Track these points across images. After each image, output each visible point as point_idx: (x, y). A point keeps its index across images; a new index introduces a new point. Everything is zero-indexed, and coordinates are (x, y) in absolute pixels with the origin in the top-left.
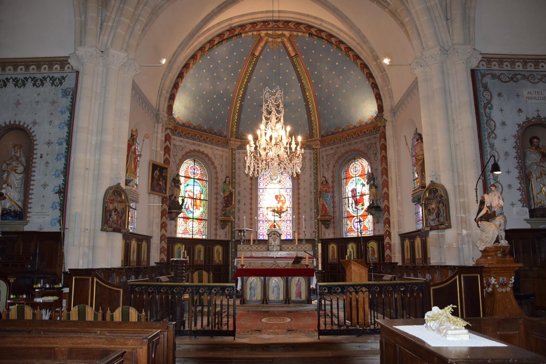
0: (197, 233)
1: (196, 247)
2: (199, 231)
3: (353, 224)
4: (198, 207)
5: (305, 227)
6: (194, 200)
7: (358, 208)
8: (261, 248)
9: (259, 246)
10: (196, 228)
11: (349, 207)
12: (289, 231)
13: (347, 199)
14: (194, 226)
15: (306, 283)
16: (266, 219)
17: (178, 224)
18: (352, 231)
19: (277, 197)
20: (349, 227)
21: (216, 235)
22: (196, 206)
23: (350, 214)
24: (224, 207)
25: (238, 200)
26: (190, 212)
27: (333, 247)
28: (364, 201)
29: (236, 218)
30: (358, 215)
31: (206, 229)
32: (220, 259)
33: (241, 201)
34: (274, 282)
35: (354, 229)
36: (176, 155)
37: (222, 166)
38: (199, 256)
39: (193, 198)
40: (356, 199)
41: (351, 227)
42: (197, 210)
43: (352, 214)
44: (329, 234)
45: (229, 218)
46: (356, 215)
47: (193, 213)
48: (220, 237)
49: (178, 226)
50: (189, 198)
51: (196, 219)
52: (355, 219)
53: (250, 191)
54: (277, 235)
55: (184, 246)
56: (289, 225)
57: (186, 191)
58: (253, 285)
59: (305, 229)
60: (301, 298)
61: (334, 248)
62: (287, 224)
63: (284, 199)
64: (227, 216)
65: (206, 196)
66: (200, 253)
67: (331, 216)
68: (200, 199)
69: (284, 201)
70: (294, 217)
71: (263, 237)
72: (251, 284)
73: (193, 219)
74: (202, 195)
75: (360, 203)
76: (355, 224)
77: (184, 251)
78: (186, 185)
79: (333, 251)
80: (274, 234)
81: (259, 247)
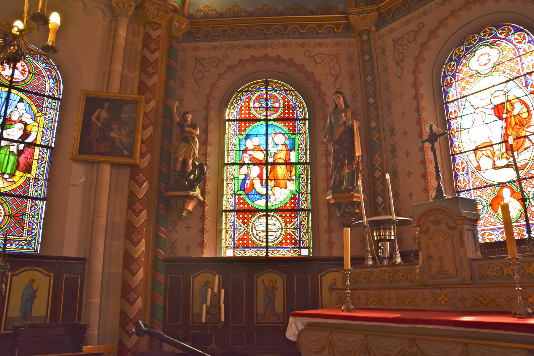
0: (281, 243)
1: (260, 279)
2: (285, 239)
4: (282, 182)
6: (269, 167)
10: (278, 234)
14: (269, 227)
16: (477, 183)
17: (223, 227)
19: (498, 110)
22: (276, 179)
31: (308, 232)
36: (201, 79)
37: (337, 77)
38: (271, 301)
49: (224, 232)
50: (254, 164)
51: (276, 211)
53: (417, 114)
54: (447, 224)
57: (245, 151)
63: (525, 110)
65: (306, 154)
66: (273, 293)
68: (287, 163)
69: (525, 115)
73: (267, 210)
74: (292, 153)
77: (216, 290)
78: (244, 136)
80: (437, 223)
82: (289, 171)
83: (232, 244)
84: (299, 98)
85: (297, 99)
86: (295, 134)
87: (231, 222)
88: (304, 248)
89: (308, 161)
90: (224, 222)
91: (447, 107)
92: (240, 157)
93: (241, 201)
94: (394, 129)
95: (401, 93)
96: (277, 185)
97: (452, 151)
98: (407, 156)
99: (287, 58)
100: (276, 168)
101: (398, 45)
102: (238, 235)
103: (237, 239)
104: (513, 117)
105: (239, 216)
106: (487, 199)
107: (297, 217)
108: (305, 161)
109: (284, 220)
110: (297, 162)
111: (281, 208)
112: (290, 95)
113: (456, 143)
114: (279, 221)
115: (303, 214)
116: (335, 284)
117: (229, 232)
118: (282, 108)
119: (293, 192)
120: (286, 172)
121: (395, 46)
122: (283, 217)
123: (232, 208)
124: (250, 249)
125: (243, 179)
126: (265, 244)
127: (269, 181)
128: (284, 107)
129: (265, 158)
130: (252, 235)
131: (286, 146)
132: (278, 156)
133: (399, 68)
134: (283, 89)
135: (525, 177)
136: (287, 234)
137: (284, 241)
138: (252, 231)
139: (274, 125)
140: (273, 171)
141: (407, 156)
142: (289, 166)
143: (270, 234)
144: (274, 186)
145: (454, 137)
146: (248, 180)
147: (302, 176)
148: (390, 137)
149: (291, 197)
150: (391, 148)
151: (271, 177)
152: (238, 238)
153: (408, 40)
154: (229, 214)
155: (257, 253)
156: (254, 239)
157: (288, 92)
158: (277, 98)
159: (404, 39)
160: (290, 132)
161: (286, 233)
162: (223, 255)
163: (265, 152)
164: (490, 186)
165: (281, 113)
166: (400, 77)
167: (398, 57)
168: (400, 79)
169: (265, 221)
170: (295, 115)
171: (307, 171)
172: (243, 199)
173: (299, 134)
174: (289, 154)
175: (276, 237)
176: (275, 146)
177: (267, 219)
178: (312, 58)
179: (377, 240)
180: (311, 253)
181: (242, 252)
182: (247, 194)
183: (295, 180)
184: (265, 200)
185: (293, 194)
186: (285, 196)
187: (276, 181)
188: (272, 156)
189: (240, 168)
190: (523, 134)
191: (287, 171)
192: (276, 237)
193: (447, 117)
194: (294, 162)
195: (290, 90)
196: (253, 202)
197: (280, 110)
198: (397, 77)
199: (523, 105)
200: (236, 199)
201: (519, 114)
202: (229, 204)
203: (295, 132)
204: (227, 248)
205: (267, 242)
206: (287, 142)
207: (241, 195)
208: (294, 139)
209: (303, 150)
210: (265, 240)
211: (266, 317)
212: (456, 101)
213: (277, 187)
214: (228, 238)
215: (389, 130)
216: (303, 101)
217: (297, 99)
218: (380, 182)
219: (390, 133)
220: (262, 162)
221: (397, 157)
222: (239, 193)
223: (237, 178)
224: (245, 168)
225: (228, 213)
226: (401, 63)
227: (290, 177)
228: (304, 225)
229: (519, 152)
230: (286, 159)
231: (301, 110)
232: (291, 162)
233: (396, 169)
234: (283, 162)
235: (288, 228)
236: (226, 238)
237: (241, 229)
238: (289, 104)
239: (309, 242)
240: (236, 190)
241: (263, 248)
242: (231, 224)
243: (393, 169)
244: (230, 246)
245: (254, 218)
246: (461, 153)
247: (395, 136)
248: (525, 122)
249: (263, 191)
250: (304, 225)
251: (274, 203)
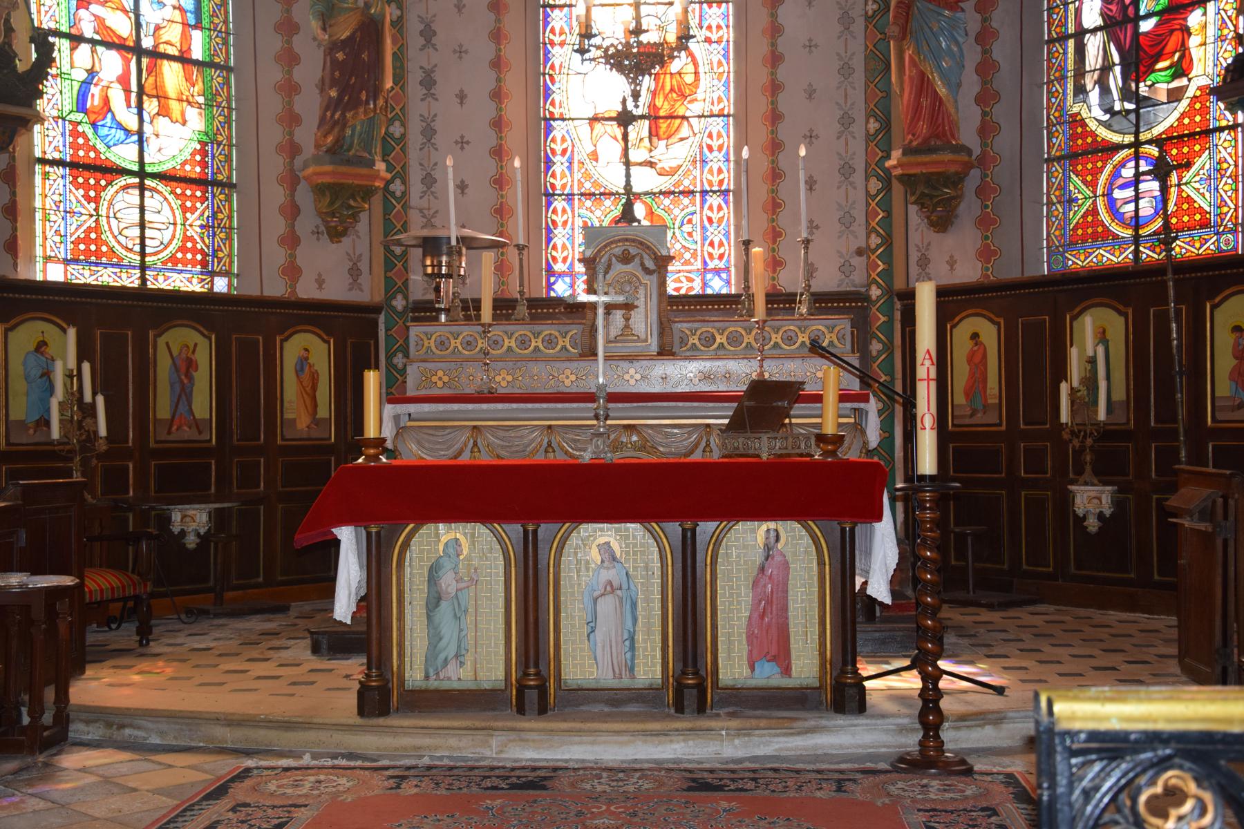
0: (173, 259)
1: (161, 341)
2: (183, 249)
3: (1108, 194)
4: (175, 106)
5: (812, 226)
6: (145, 61)
7: (1143, 90)
8: (550, 342)
9: (537, 328)
10: (167, 235)
11: (1080, 90)
12: (716, 252)
13: (1071, 43)
14: (148, 217)
15: (821, 563)
16: (588, 185)
17: (38, 203)
18: (1095, 236)
20: (1076, 216)
21: (292, 271)
22: (161, 97)
23: (1084, 135)
24: (333, 105)
25: (419, 75)
26: (120, 134)
27: (975, 336)
28: (1193, 42)
29: (415, 176)
30: (1142, 137)
31: (230, 239)
32: (323, 413)
33: (437, 76)
34: (595, 555)
35: (1115, 228)
38: (184, 393)
39: (138, 51)
40: (1136, 32)
41: (1094, 211)
42: (162, 122)
43: (1104, 133)
44: (952, 263)
45: (364, 171)
46: (1129, 139)
47: (141, 142)
48: (320, 282)
49: (39, 215)
50: (109, 45)
51: (163, 177)
52: (1123, 164)
54: (642, 264)
55: (72, 332)
56: (715, 216)
58: (448, 582)
59: (811, 233)
60: (787, 671)
61: (983, 338)
62: (706, 212)
63: (691, 68)
64: (349, 162)
65: (225, 42)
67: (969, 152)
68: (183, 59)
69: (689, 79)
70: (745, 153)
71: (572, 286)
72: (434, 573)
75: (1159, 57)
76: (1118, 194)
79: (977, 359)
80: (626, 259)
81: (536, 335)
83: (62, 250)
87: (57, 192)
88: (220, 274)
89: (232, 63)
90: (38, 190)
91: (546, 16)
92: (72, 17)
93: (81, 141)
94: (435, 33)
97: (545, 110)
98: (461, 103)
102: (77, 226)
103: (73, 239)
104: (668, 77)
105: (75, 178)
106: (603, 218)
107: (207, 199)
109: (180, 202)
110: (208, 59)
111: (172, 173)
113: (556, 97)
114: (169, 204)
115: (221, 193)
116: (307, 359)
117: (53, 218)
120: (184, 83)
122: (177, 196)
123: (57, 156)
124: (106, 266)
125: (82, 82)
126: (138, 258)
127: (145, 98)
129: (134, 32)
130: (108, 233)
135: (672, 189)
136: (186, 238)
137: (179, 255)
138: (108, 222)
140: (154, 74)
141: (461, 103)
143: (148, 233)
144: (158, 114)
145: (553, 82)
146: (96, 85)
147: (219, 99)
148: (421, 50)
151: (148, 87)
152: (76, 236)
154: (51, 170)
155: (120, 277)
156: (113, 243)
161: (185, 234)
162: (39, 277)
163: (132, 15)
164: (611, 194)
169: (137, 200)
171: (229, 88)
172: (84, 135)
175: (162, 243)
177: (142, 196)
179: (433, 274)
180: (235, 289)
181: (87, 273)
182: (94, 125)
184: (136, 147)
186: (182, 144)
187: (163, 100)
188: (151, 33)
189: (73, 49)
190: (681, 112)
192: (162, 243)
193: (544, 37)
196: (109, 147)
199: (690, 59)
200: (67, 133)
201: (680, 73)
202: (50, 143)
204: (48, 259)
205: (143, 254)
207: (79, 123)
209: (220, 31)
210: (137, 248)
211: (174, 428)
212: (566, 9)
214: (49, 234)
215: (421, 33)
219: (422, 41)
220: (127, 43)
222: (73, 117)
223: (66, 76)
224: (84, 48)
225: (47, 168)
228: (222, 220)
229: (670, 141)
233: (432, 124)
234: (177, 53)
236: (44, 233)
237: (82, 214)
239: (231, 262)
240: (67, 109)
241: (134, 267)
242: (56, 198)
243: (424, 124)
244: (56, 257)
245: (111, 190)
246: (563, 119)
248: (687, 91)
249: (131, 122)
250: (222, 220)
251: (157, 160)
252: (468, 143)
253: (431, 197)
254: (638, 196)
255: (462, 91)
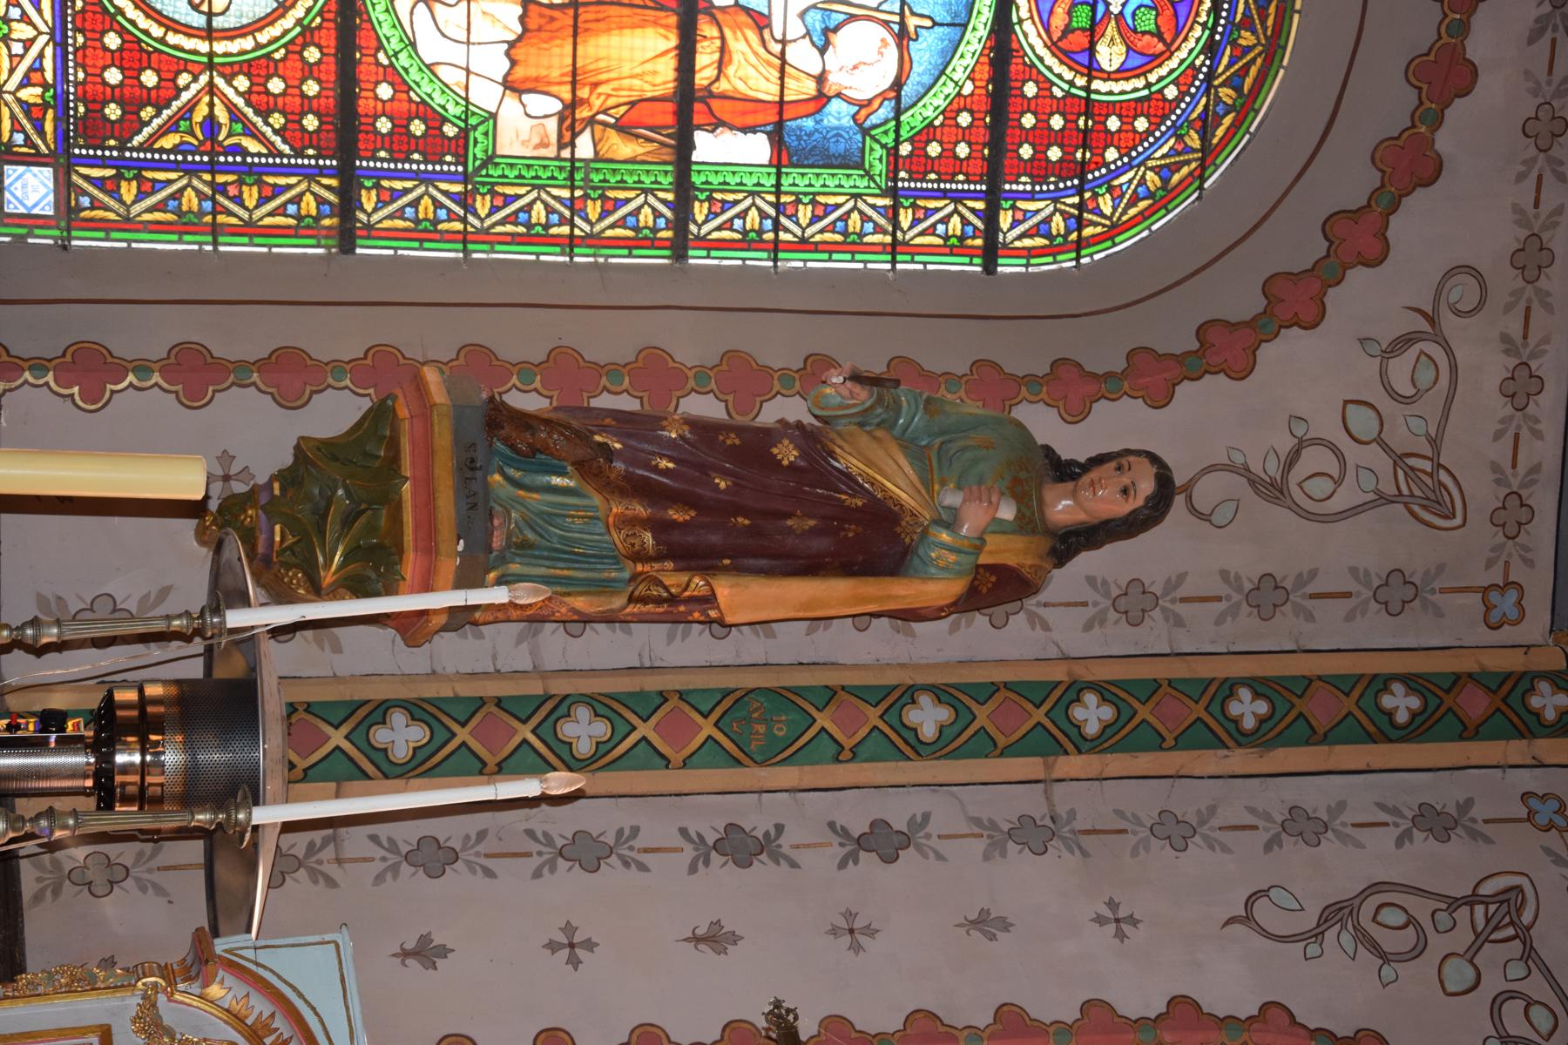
31: (183, 226)
33: (763, 869)
37: (1275, 491)
65: (747, 242)
74: (757, 148)
82: (634, 115)
84: (1144, 216)
85: (1143, 205)
86: (893, 175)
88: (64, 187)
94: (889, 859)
95: (1133, 921)
96: (533, 23)
98: (696, 939)
99: (1444, 142)
100: (656, 23)
101: (1480, 924)
107: (299, 153)
108: (697, 237)
110: (697, 179)
111: (363, 39)
112: (1173, 152)
115: (320, 201)
118: (1087, 89)
119: (478, 134)
120: (625, 96)
121: (1472, 900)
122: (295, 48)
128: (1089, 106)
131: (811, 107)
132: (742, 45)
133: (1309, 921)
134: (1218, 100)
136: (172, 66)
137: (112, 41)
139: (965, 26)
141: (696, 939)
142: (669, 119)
147: (594, 210)
148: (832, 825)
149: (445, 120)
150: (759, 834)
153: (1512, 995)
157: (1194, 140)
158: (1156, 60)
159: (1517, 970)
160: (911, 140)
165: (1045, 85)
166: (1248, 919)
167: (1393, 917)
168: (1231, 921)
170: (1024, 184)
171: (629, 245)
173: (887, 202)
174: (750, 120)
176: (819, 26)
178: (1426, 327)
183: (566, 153)
185: (464, 134)
187: (566, 19)
191: (633, 104)
194: (695, 157)
195: (1208, 155)
197: (1068, 75)
198: (1250, 902)
203: (902, 174)
206: (838, 114)
208: (860, 166)
209: (777, 226)
213: (523, 19)
215: (878, 825)
216: (1125, 242)
217: (1143, 205)
218: (525, 741)
219: (859, 827)
221: (693, 869)
226: (1346, 938)
227: (591, 121)
228: (239, 200)
230: (723, 96)
231: (1058, 223)
232: (700, 137)
233: (614, 859)
234: (703, 77)
235: (220, 82)
238: (1109, 139)
239: (105, 227)
243: (610, 840)
247: (842, 865)
250: (239, 200)
252: (574, 962)
253: (378, 866)
254: (596, 153)
255: (735, 938)
